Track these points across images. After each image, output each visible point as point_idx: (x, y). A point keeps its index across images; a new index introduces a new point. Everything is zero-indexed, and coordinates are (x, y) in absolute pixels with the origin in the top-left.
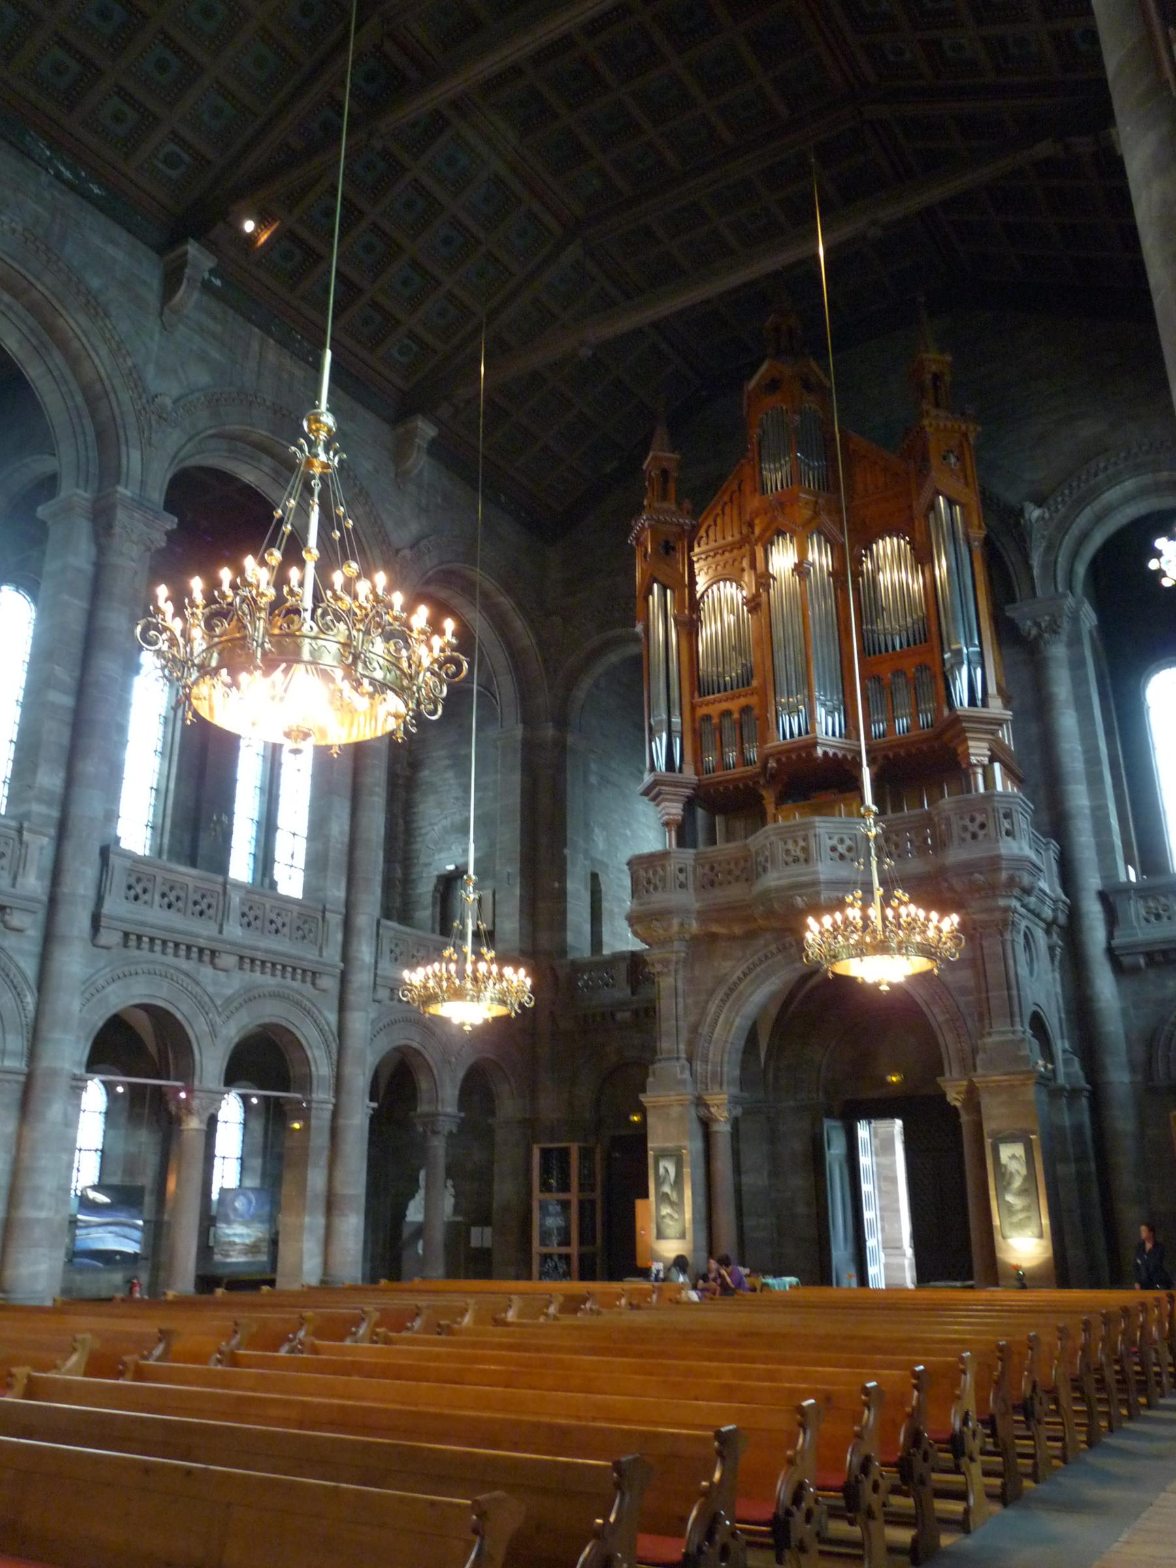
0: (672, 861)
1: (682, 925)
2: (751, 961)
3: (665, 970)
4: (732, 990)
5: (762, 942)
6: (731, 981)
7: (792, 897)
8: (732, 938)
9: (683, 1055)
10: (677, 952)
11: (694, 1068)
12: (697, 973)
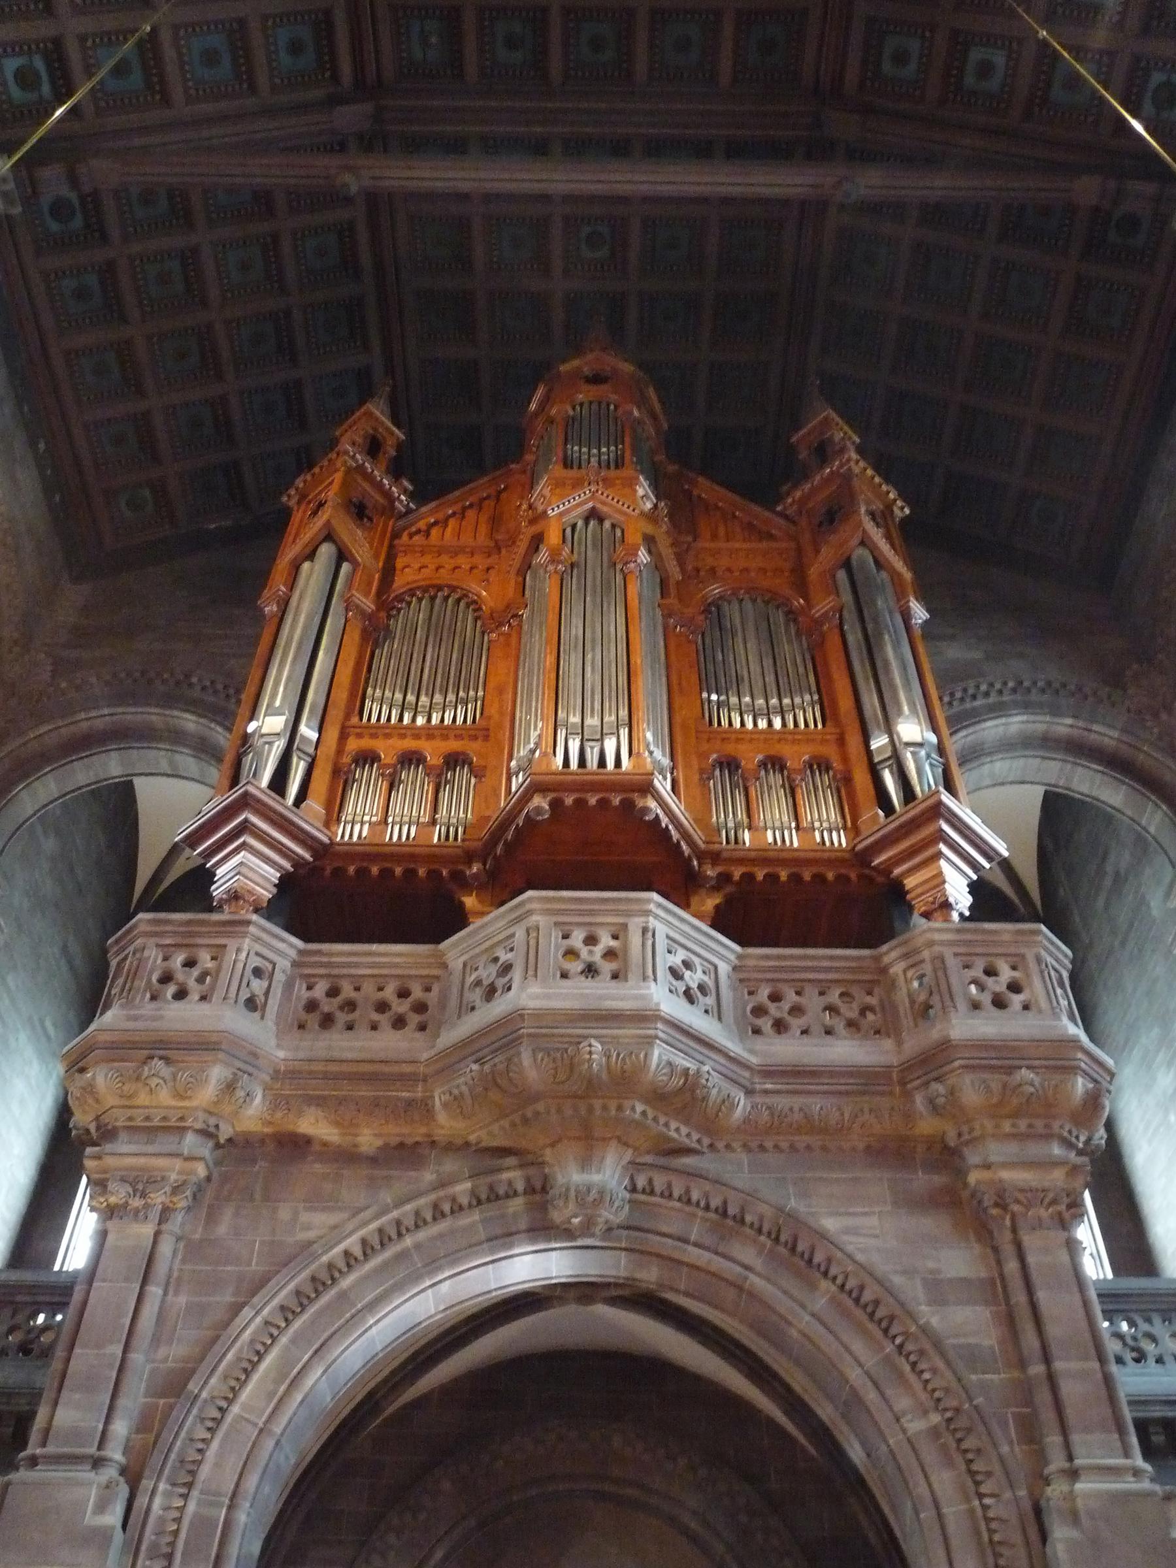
0: (247, 943)
1: (230, 1087)
2: (395, 1214)
3: (137, 1203)
4: (318, 1285)
5: (429, 1176)
6: (325, 1259)
7: (578, 1041)
8: (347, 1157)
10: (190, 1159)
11: (141, 1501)
12: (222, 1229)
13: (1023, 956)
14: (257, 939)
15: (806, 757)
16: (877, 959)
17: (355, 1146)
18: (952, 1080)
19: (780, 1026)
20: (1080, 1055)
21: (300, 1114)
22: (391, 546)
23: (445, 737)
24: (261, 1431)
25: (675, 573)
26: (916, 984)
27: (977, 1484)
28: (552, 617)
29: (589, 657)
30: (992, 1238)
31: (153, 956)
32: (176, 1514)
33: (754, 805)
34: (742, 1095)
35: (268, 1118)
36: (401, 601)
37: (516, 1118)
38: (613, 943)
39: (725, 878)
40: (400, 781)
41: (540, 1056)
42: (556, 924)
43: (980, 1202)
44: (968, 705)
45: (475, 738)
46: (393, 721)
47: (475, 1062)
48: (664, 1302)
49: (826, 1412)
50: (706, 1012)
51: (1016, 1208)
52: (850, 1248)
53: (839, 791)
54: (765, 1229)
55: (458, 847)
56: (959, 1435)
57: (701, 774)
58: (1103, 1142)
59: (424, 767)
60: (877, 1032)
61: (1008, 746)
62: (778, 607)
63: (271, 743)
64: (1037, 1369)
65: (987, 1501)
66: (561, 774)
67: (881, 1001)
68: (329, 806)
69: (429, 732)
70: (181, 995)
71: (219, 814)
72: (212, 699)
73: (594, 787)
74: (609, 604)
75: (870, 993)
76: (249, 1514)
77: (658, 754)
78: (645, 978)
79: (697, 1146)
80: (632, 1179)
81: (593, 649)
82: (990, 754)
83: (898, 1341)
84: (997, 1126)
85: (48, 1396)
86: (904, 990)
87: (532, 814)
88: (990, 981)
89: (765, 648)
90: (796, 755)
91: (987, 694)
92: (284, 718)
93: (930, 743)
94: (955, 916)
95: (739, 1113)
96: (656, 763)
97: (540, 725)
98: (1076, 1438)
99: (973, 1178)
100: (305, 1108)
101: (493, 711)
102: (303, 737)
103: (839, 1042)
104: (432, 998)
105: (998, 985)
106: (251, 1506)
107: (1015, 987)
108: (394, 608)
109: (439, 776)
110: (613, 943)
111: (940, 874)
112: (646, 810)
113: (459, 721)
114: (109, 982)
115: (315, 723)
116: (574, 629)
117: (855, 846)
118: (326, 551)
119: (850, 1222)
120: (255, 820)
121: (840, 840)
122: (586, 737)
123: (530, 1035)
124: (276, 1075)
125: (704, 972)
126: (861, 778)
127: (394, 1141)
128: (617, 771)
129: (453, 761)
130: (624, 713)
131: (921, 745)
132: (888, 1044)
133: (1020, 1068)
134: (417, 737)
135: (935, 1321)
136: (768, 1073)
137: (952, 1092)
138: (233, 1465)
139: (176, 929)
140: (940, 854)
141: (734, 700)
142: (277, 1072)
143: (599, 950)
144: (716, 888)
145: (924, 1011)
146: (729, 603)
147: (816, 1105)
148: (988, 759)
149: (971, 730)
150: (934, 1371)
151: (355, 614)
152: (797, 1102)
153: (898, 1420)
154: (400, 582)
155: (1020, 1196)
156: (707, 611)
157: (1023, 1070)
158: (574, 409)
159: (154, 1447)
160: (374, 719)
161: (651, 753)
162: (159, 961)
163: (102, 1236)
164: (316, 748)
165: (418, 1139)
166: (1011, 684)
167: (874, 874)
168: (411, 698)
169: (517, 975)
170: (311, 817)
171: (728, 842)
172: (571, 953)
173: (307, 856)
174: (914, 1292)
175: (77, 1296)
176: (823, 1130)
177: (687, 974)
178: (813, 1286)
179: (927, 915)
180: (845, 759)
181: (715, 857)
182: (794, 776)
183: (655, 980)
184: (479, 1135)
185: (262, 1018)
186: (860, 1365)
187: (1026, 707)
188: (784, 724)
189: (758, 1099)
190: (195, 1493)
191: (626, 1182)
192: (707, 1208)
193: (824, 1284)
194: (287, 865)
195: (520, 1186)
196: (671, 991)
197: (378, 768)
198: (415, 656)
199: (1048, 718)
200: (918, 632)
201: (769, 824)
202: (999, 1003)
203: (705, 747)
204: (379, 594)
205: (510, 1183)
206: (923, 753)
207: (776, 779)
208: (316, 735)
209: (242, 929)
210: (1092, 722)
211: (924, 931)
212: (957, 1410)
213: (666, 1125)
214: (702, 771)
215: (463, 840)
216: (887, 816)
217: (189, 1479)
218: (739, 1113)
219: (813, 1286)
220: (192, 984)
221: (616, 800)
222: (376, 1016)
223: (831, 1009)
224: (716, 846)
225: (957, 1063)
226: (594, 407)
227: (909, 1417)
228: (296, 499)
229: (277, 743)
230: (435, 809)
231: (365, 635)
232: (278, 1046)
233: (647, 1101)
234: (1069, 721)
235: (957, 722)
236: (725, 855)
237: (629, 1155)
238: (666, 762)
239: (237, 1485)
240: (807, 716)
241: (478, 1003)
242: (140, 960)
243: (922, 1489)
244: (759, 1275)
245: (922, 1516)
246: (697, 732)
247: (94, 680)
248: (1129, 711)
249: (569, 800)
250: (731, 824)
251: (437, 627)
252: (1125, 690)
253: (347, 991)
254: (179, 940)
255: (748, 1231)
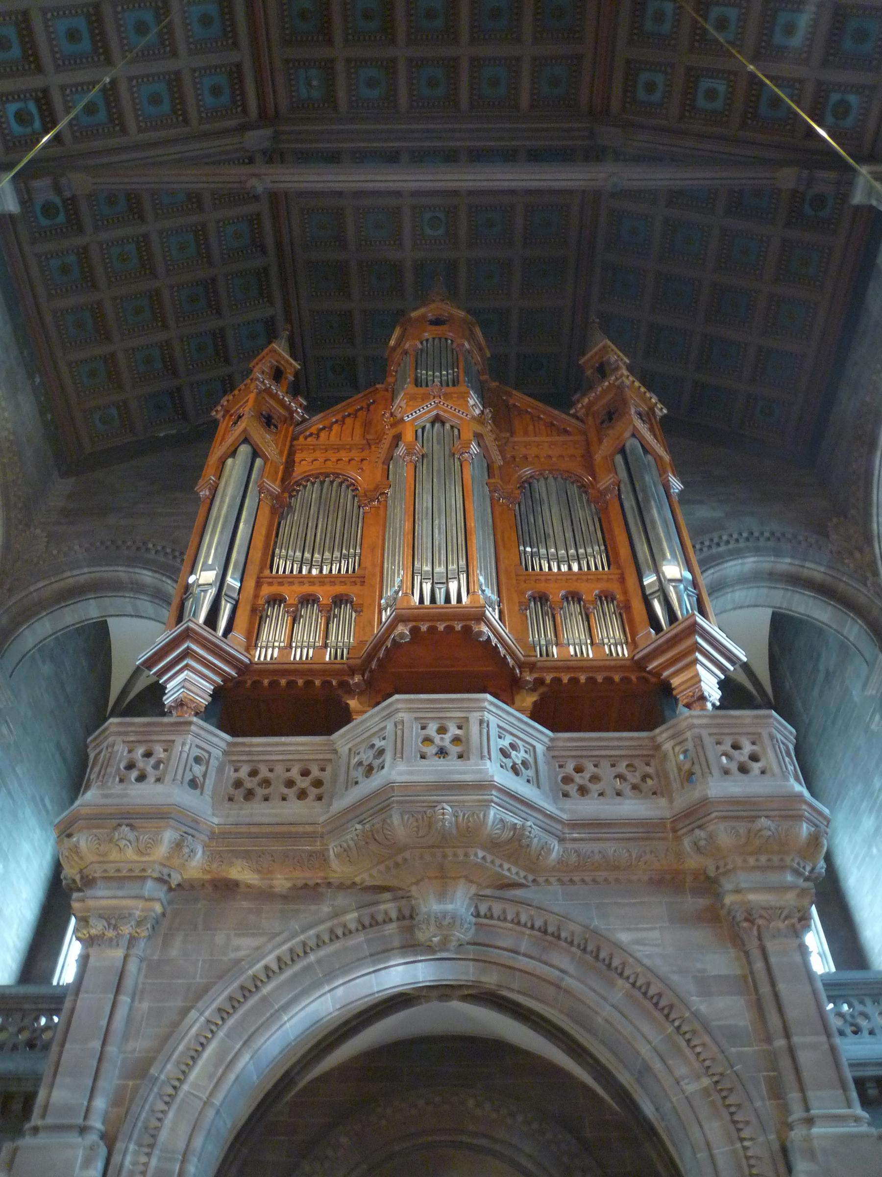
1: (178, 845)
3: (111, 934)
4: (246, 992)
5: (326, 909)
6: (250, 972)
8: (265, 895)
9: (97, 1123)
12: (174, 952)
13: (760, 734)
14: (197, 735)
15: (597, 592)
16: (653, 739)
17: (271, 887)
18: (711, 827)
19: (583, 791)
20: (804, 807)
21: (231, 864)
22: (291, 446)
23: (333, 583)
24: (205, 1103)
25: (499, 461)
26: (682, 757)
27: (739, 1130)
28: (409, 495)
29: (436, 522)
30: (744, 945)
31: (121, 750)
32: (141, 1168)
33: (559, 628)
34: (556, 843)
35: (207, 868)
36: (299, 485)
37: (390, 863)
38: (458, 732)
39: (540, 682)
40: (301, 616)
41: (406, 817)
42: (416, 719)
43: (734, 918)
44: (714, 550)
45: (355, 583)
46: (295, 573)
47: (359, 823)
48: (504, 998)
49: (624, 1078)
50: (528, 781)
51: (760, 922)
52: (639, 955)
53: (621, 614)
54: (576, 942)
55: (343, 664)
56: (724, 1094)
57: (520, 606)
58: (823, 870)
59: (318, 605)
60: (654, 793)
61: (744, 580)
62: (573, 483)
63: (205, 591)
64: (780, 1043)
65: (746, 1144)
66: (418, 608)
67: (657, 771)
68: (248, 636)
69: (322, 580)
70: (142, 778)
71: (167, 645)
72: (163, 559)
73: (441, 617)
74: (450, 484)
75: (648, 764)
76: (197, 1167)
77: (488, 592)
78: (482, 757)
79: (523, 881)
80: (476, 907)
81: (439, 517)
82: (732, 585)
83: (677, 1024)
84: (745, 861)
85: (46, 1080)
86: (674, 763)
87: (398, 639)
88: (736, 753)
89: (565, 512)
90: (591, 592)
91: (728, 542)
92: (215, 572)
93: (687, 579)
94: (709, 706)
95: (554, 855)
96: (487, 598)
97: (402, 572)
98: (811, 1094)
99: (728, 900)
100: (234, 860)
101: (367, 563)
102: (229, 586)
103: (627, 802)
104: (326, 776)
105: (743, 756)
106: (199, 1160)
107: (754, 758)
108: (294, 490)
109: (329, 611)
110: (458, 732)
111: (697, 675)
112: (481, 633)
113: (343, 571)
114: (88, 770)
115: (238, 575)
116: (424, 503)
117: (634, 656)
118: (244, 449)
119: (640, 935)
120: (194, 647)
121: (623, 652)
122: (435, 581)
123: (398, 802)
124: (213, 836)
125: (526, 752)
126: (637, 605)
127: (300, 883)
128: (459, 605)
129: (340, 600)
130: (462, 563)
131: (680, 581)
132: (663, 802)
133: (760, 817)
134: (312, 583)
135: (703, 1008)
136: (574, 825)
137: (711, 837)
138: (184, 1129)
139: (138, 729)
140: (696, 661)
141: (543, 551)
142: (213, 833)
143: (448, 737)
144: (534, 690)
145: (689, 777)
146: (538, 480)
147: (611, 848)
148: (731, 589)
149: (717, 568)
150: (704, 1045)
151: (266, 496)
152: (596, 846)
153: (678, 1083)
154: (299, 471)
155: (763, 913)
156: (522, 487)
157: (763, 819)
158: (422, 343)
159: (126, 1117)
160: (281, 572)
161: (483, 591)
162: (125, 754)
163: (84, 961)
164: (239, 594)
165: (319, 881)
166: (745, 535)
167: (649, 677)
168: (307, 555)
169: (388, 757)
170: (235, 644)
171: (541, 655)
172: (428, 740)
173: (233, 673)
174: (686, 986)
175: (67, 1005)
176: (617, 868)
177: (513, 753)
178: (611, 984)
179: (688, 706)
180: (625, 592)
181: (532, 667)
182: (588, 605)
183: (490, 759)
184: (364, 878)
185: (202, 793)
186: (649, 1042)
187: (757, 551)
188: (580, 568)
189: (569, 845)
190: (156, 1152)
191: (472, 909)
192: (532, 927)
193: (620, 982)
194: (219, 680)
195: (394, 915)
196: (502, 766)
197: (284, 607)
198: (310, 524)
199: (773, 559)
200: (675, 499)
201: (571, 641)
202: (743, 769)
203: (523, 586)
204: (283, 480)
205: (386, 913)
206: (682, 587)
207: (575, 608)
208: (239, 585)
209: (186, 728)
210: (805, 560)
211: (687, 718)
212: (722, 1074)
213: (501, 866)
214: (520, 603)
215: (347, 659)
216: (657, 633)
217: (151, 1141)
218: (554, 855)
219: (611, 984)
220: (149, 770)
221: (458, 627)
222: (285, 791)
223: (620, 777)
224: (533, 659)
225: (713, 815)
226: (437, 341)
227: (686, 1081)
228: (222, 413)
229: (210, 591)
230: (327, 636)
231: (273, 511)
232: (214, 815)
233: (484, 848)
234: (788, 560)
235: (706, 563)
236: (539, 664)
237: (473, 889)
238: (494, 598)
239: (188, 1146)
240: (596, 561)
241: (360, 779)
242: (111, 753)
243: (696, 1134)
244: (571, 976)
245: (699, 1156)
246: (517, 575)
247: (77, 547)
248: (831, 552)
249: (424, 628)
250: (543, 642)
251: (325, 505)
252: (827, 536)
253: (264, 772)
254: (140, 738)
255: (563, 944)
